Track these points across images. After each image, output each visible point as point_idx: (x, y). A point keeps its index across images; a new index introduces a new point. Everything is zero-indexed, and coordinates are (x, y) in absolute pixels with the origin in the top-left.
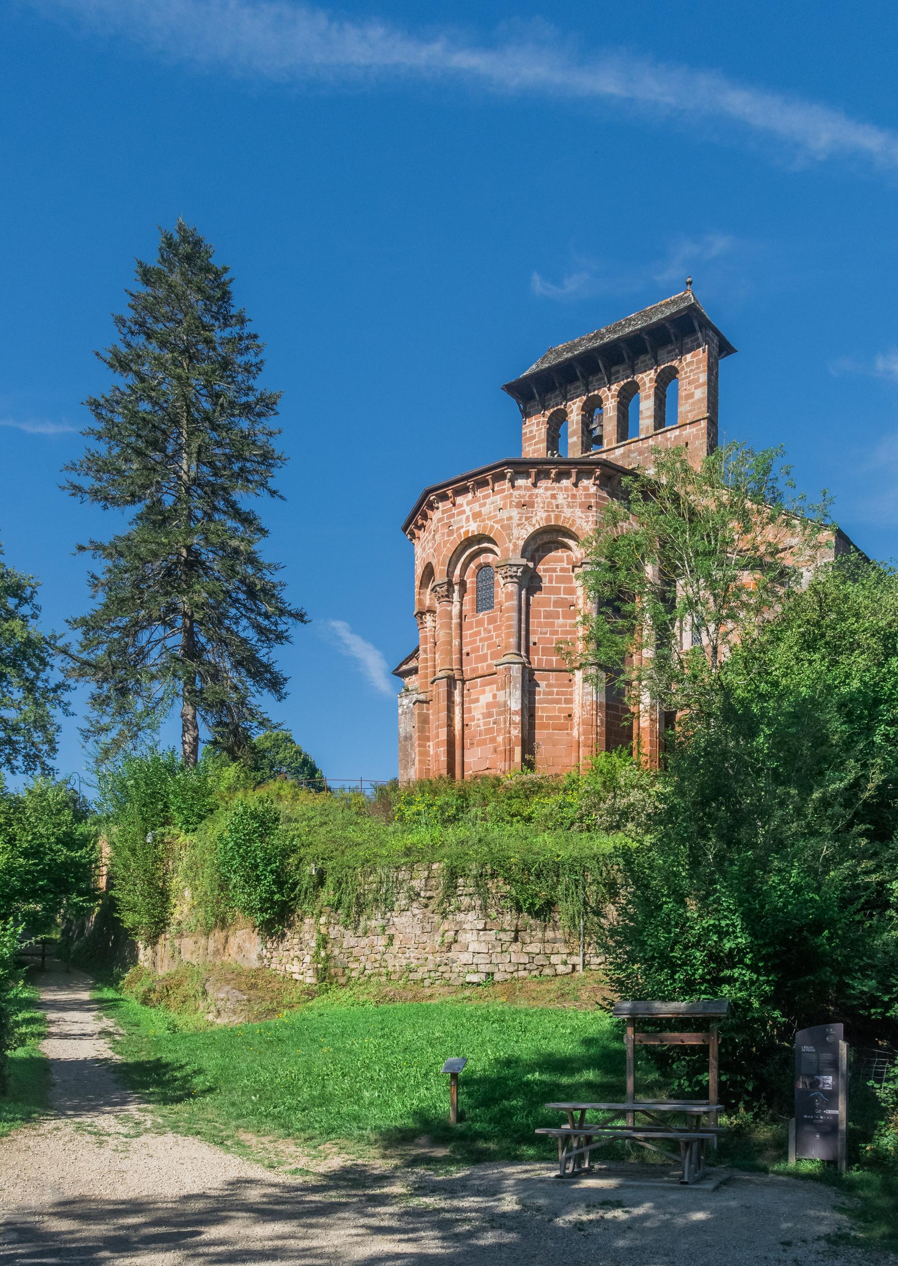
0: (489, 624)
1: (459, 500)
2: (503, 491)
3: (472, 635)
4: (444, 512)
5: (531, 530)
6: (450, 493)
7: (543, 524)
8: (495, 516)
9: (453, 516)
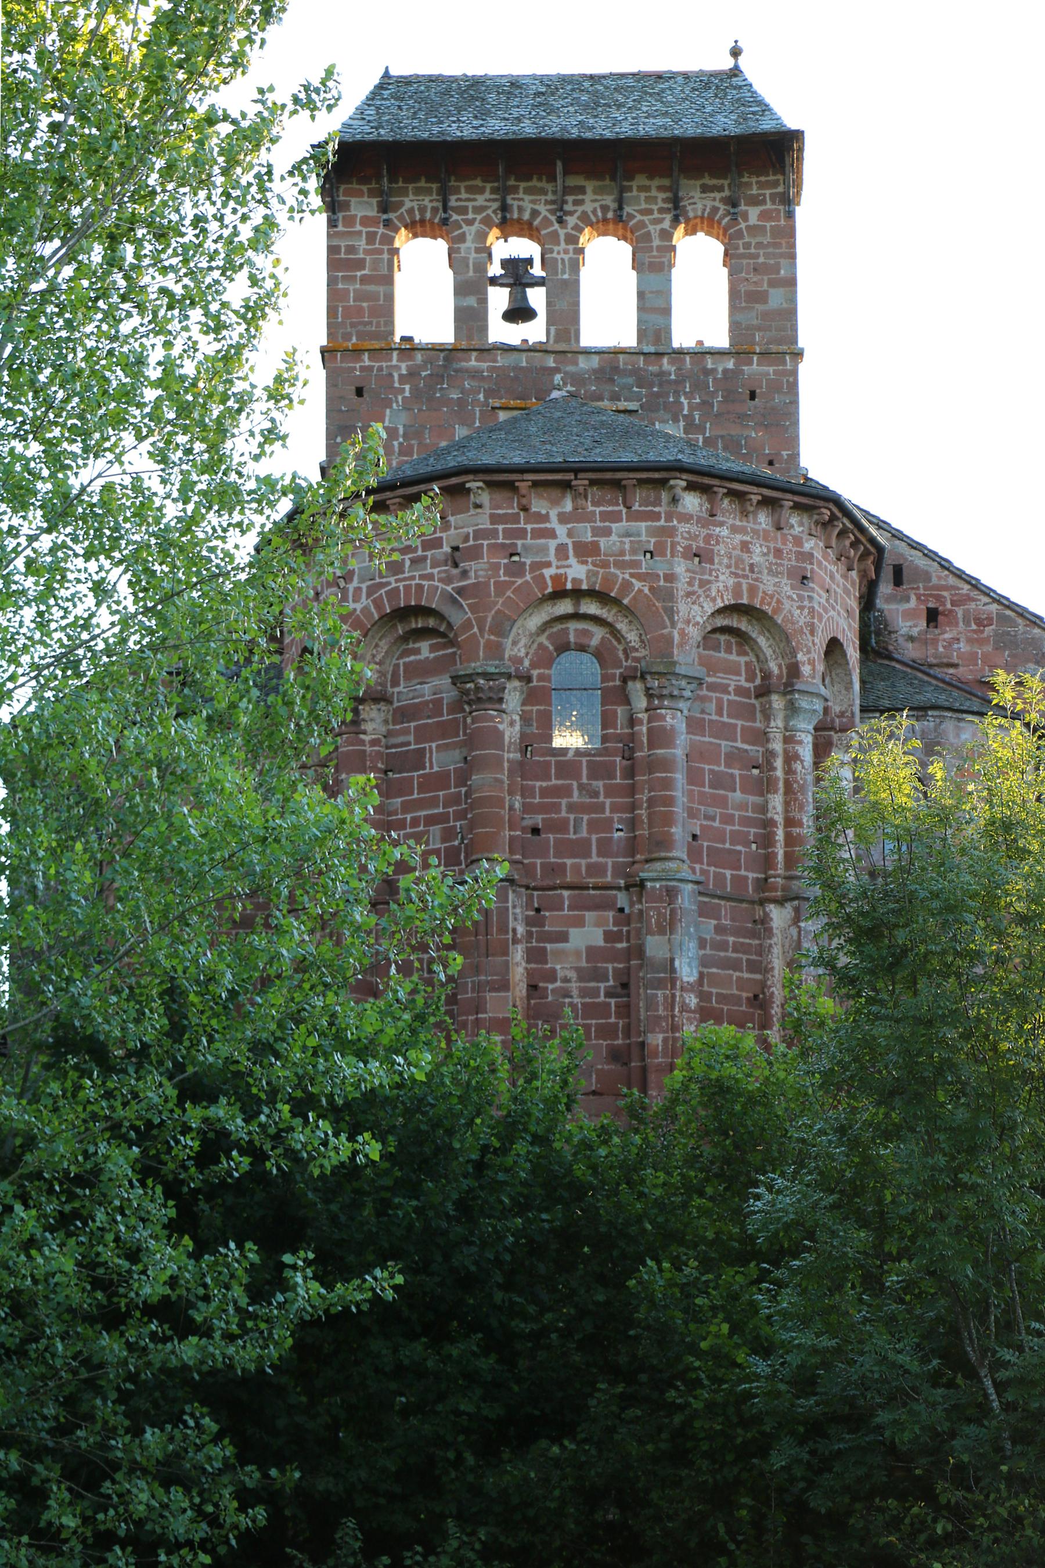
0: (593, 775)
1: (538, 505)
2: (656, 516)
3: (545, 792)
4: (495, 519)
5: (709, 608)
6: (523, 486)
7: (729, 600)
8: (636, 564)
9: (522, 534)
